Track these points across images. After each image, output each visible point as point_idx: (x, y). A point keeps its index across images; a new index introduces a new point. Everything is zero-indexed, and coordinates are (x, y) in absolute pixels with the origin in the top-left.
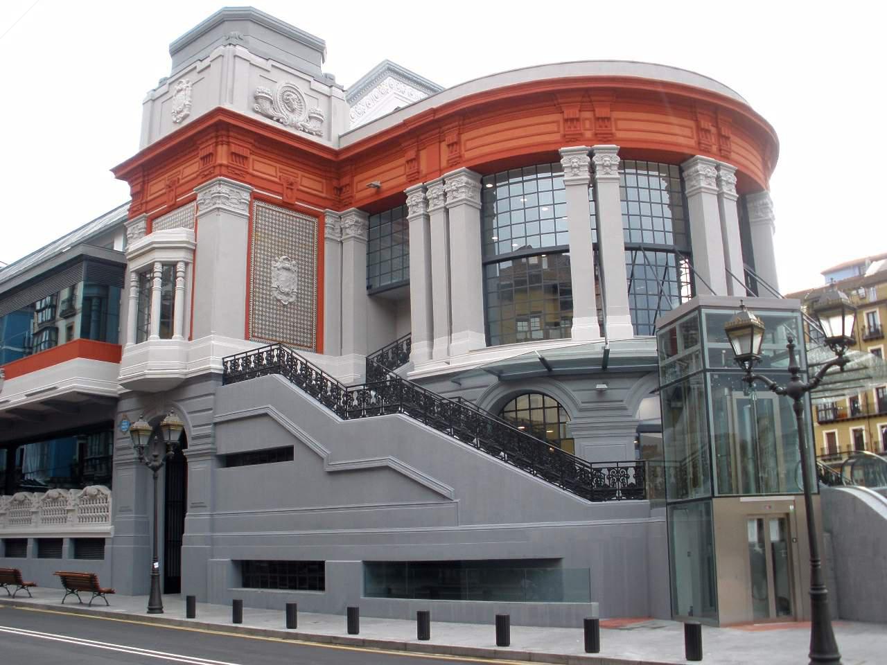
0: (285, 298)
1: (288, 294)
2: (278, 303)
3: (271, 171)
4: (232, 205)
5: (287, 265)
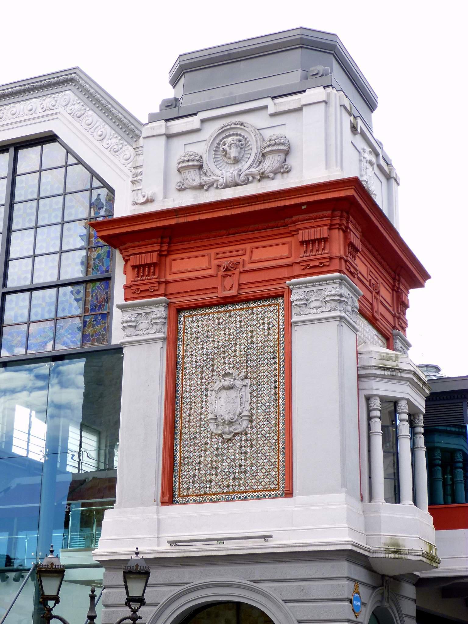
0: (227, 430)
1: (231, 423)
2: (220, 439)
3: (202, 262)
5: (227, 382)
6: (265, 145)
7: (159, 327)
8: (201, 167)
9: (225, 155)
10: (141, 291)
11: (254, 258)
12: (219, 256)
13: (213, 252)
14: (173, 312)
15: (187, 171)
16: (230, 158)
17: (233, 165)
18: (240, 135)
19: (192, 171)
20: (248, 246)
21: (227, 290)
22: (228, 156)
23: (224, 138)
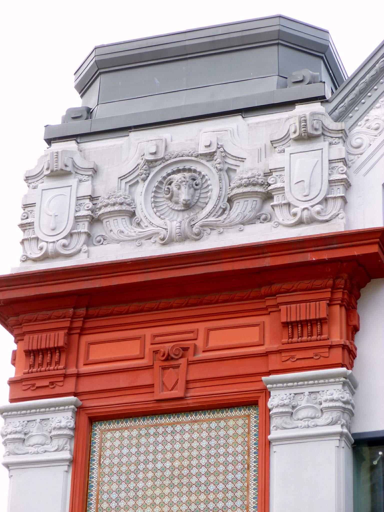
4: (33, 449)
6: (232, 185)
7: (61, 442)
8: (133, 214)
9: (170, 199)
10: (38, 388)
11: (212, 344)
12: (158, 339)
13: (148, 333)
14: (84, 420)
15: (111, 220)
16: (177, 203)
17: (181, 214)
18: (195, 171)
19: (119, 219)
20: (202, 327)
21: (168, 390)
22: (174, 199)
23: (169, 175)
